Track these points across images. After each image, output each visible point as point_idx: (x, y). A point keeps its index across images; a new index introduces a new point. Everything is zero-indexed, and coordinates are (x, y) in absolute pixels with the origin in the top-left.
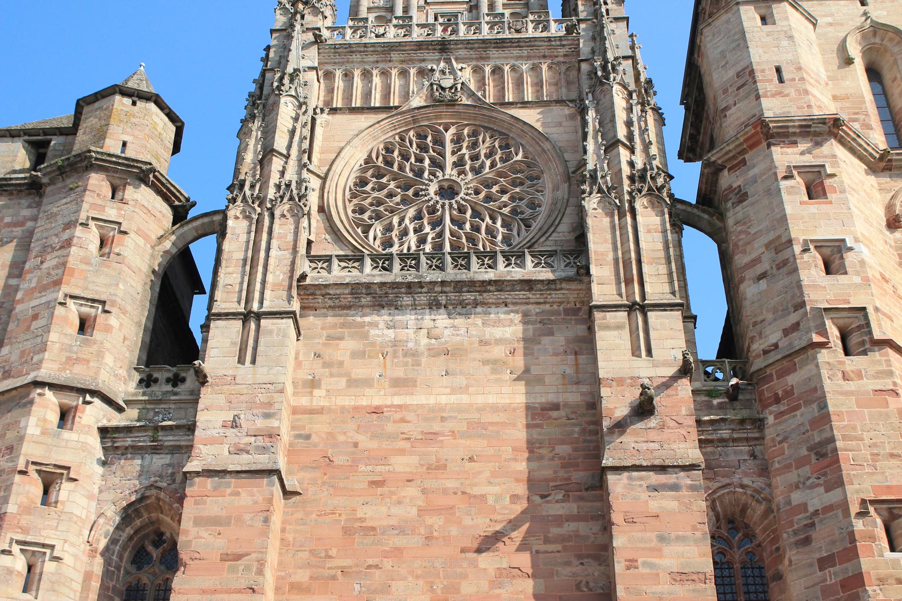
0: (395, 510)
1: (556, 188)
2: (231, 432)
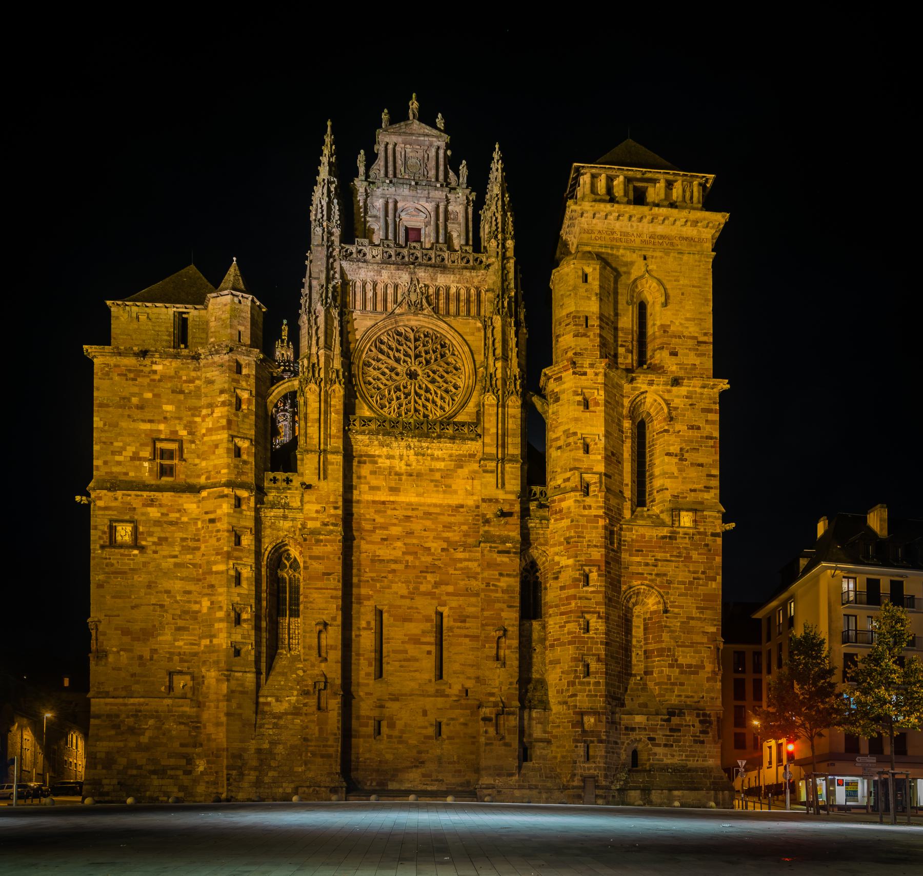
0: (393, 552)
2: (319, 516)
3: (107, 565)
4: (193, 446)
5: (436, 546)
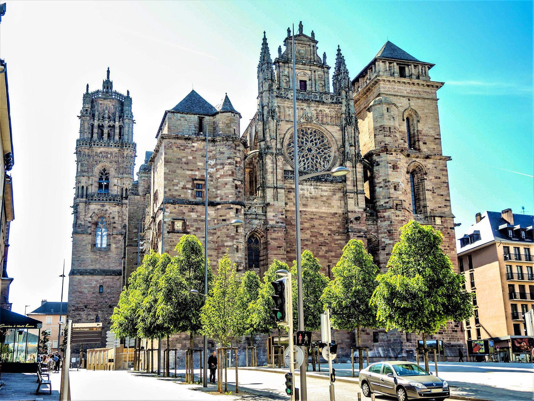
0: (306, 236)
1: (335, 152)
3: (170, 242)
4: (212, 182)
5: (326, 233)
